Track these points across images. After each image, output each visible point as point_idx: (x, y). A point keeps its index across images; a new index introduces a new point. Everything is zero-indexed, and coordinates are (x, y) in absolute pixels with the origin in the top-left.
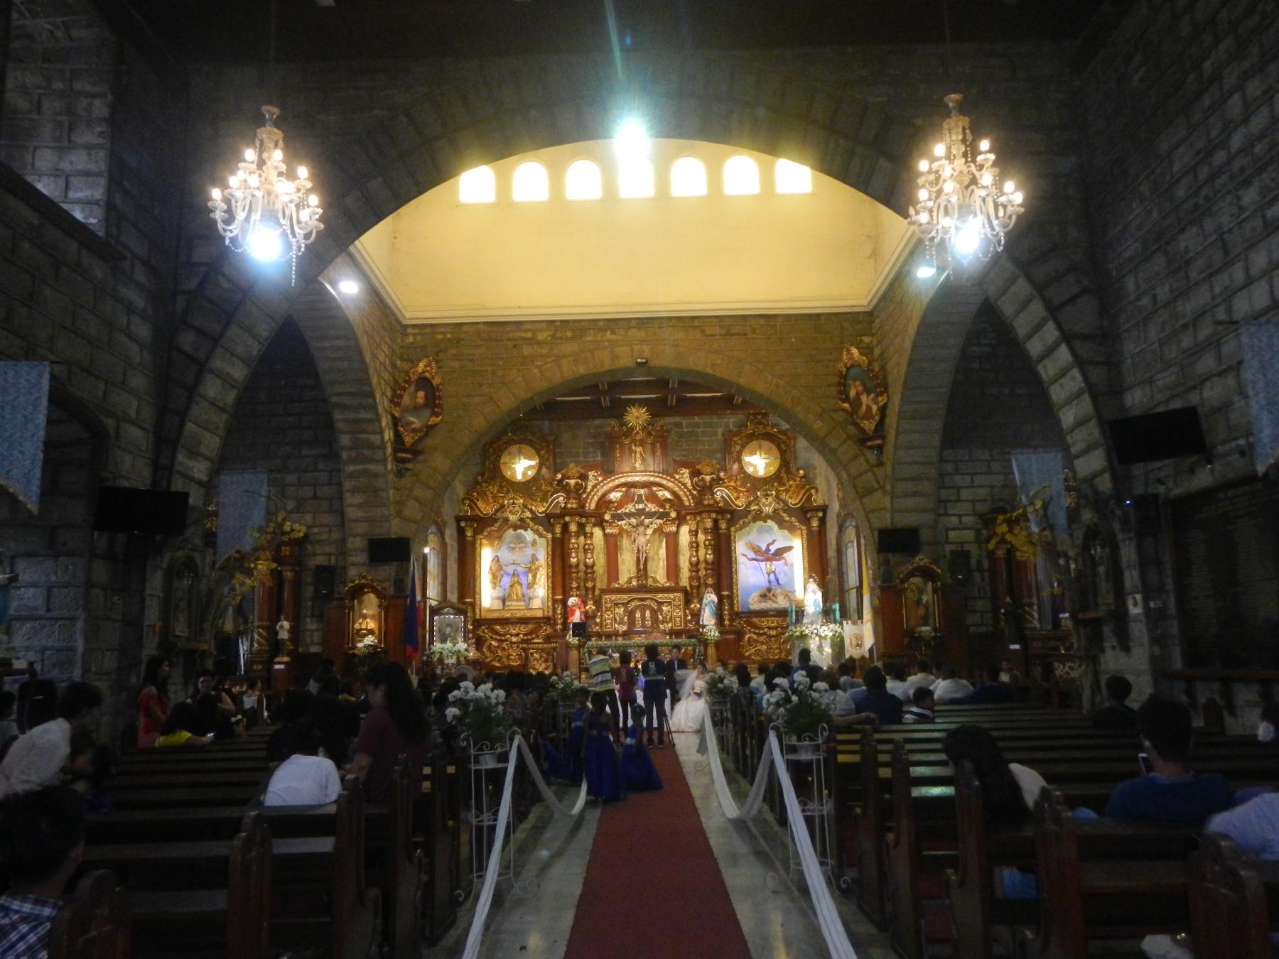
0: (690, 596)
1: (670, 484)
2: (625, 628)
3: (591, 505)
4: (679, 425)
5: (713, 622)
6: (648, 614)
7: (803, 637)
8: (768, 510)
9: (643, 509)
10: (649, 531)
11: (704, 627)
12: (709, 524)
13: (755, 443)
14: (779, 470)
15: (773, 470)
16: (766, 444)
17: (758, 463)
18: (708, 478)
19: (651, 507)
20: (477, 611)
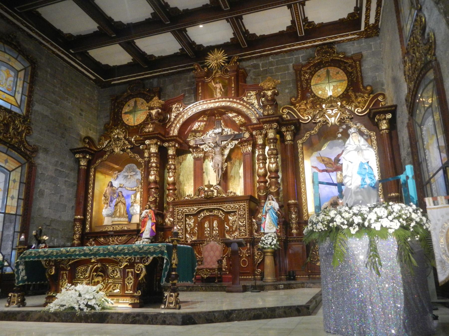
0: (253, 204)
1: (239, 106)
2: (194, 238)
3: (174, 132)
4: (256, 66)
5: (274, 230)
6: (215, 223)
7: (333, 231)
8: (332, 121)
9: (222, 133)
10: (227, 152)
11: (264, 234)
12: (271, 135)
13: (323, 71)
14: (347, 90)
15: (340, 91)
16: (333, 70)
17: (328, 88)
18: (269, 93)
19: (228, 131)
20: (88, 226)
